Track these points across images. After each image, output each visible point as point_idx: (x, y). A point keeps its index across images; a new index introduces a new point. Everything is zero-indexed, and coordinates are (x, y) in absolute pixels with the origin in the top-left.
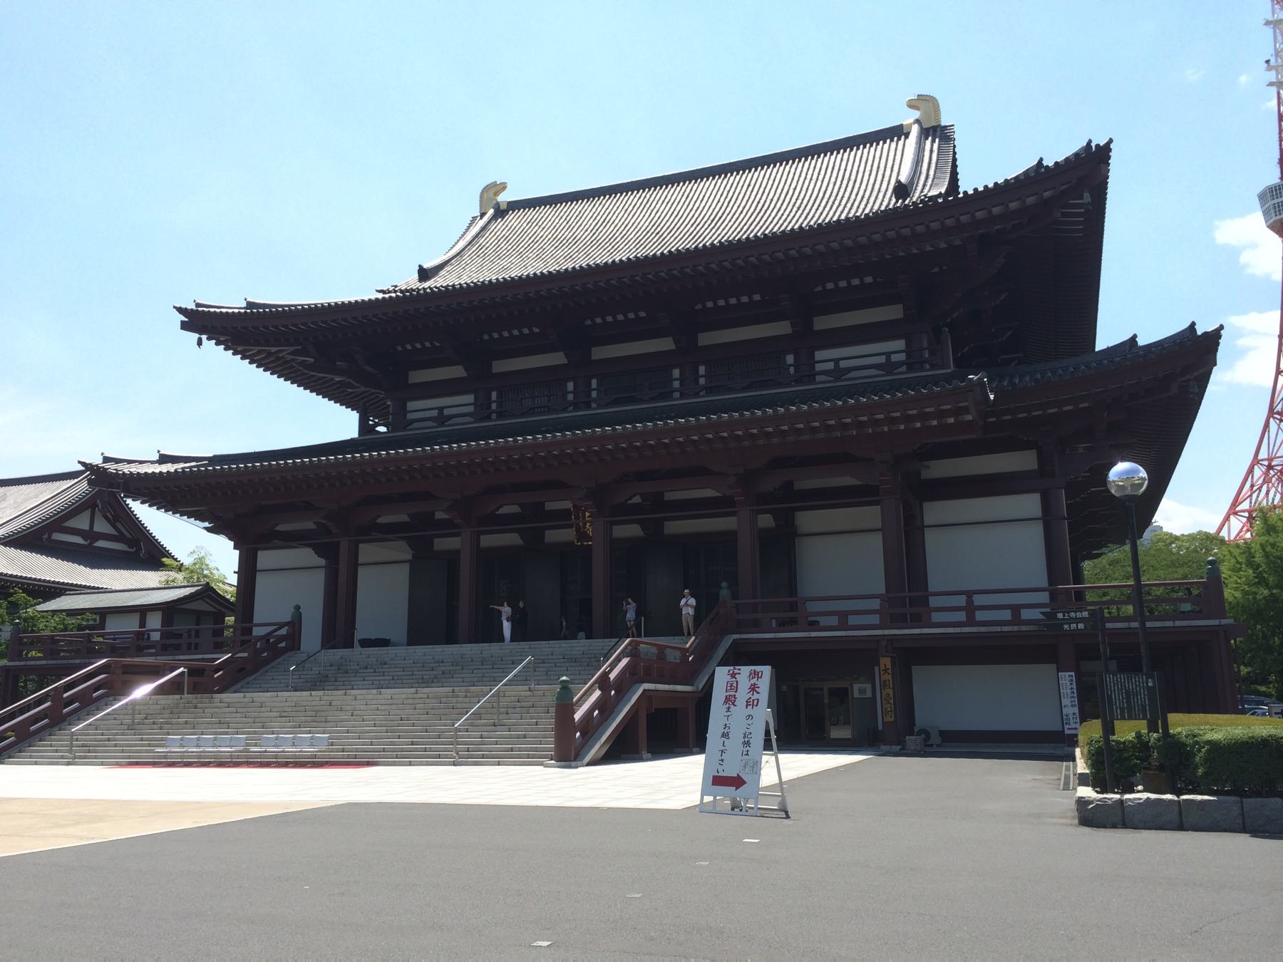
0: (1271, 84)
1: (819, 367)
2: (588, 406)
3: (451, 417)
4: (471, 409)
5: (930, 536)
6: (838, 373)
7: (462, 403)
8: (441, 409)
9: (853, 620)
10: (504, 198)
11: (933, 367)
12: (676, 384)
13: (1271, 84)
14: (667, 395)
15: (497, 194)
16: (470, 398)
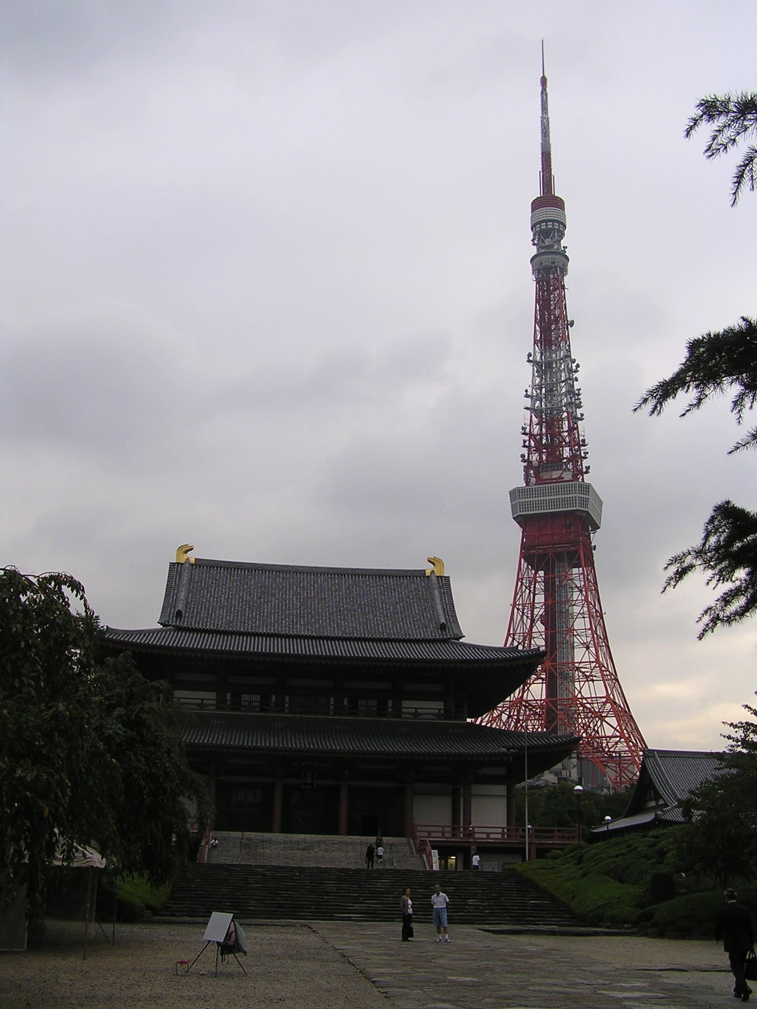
0: (527, 408)
1: (404, 710)
2: (283, 711)
3: (208, 705)
4: (214, 702)
5: (474, 801)
6: (416, 715)
7: (210, 696)
8: (202, 700)
9: (433, 834)
10: (192, 556)
11: (456, 718)
12: (332, 707)
13: (527, 408)
14: (328, 713)
15: (186, 552)
16: (212, 695)
